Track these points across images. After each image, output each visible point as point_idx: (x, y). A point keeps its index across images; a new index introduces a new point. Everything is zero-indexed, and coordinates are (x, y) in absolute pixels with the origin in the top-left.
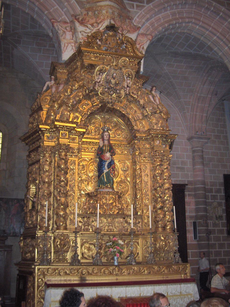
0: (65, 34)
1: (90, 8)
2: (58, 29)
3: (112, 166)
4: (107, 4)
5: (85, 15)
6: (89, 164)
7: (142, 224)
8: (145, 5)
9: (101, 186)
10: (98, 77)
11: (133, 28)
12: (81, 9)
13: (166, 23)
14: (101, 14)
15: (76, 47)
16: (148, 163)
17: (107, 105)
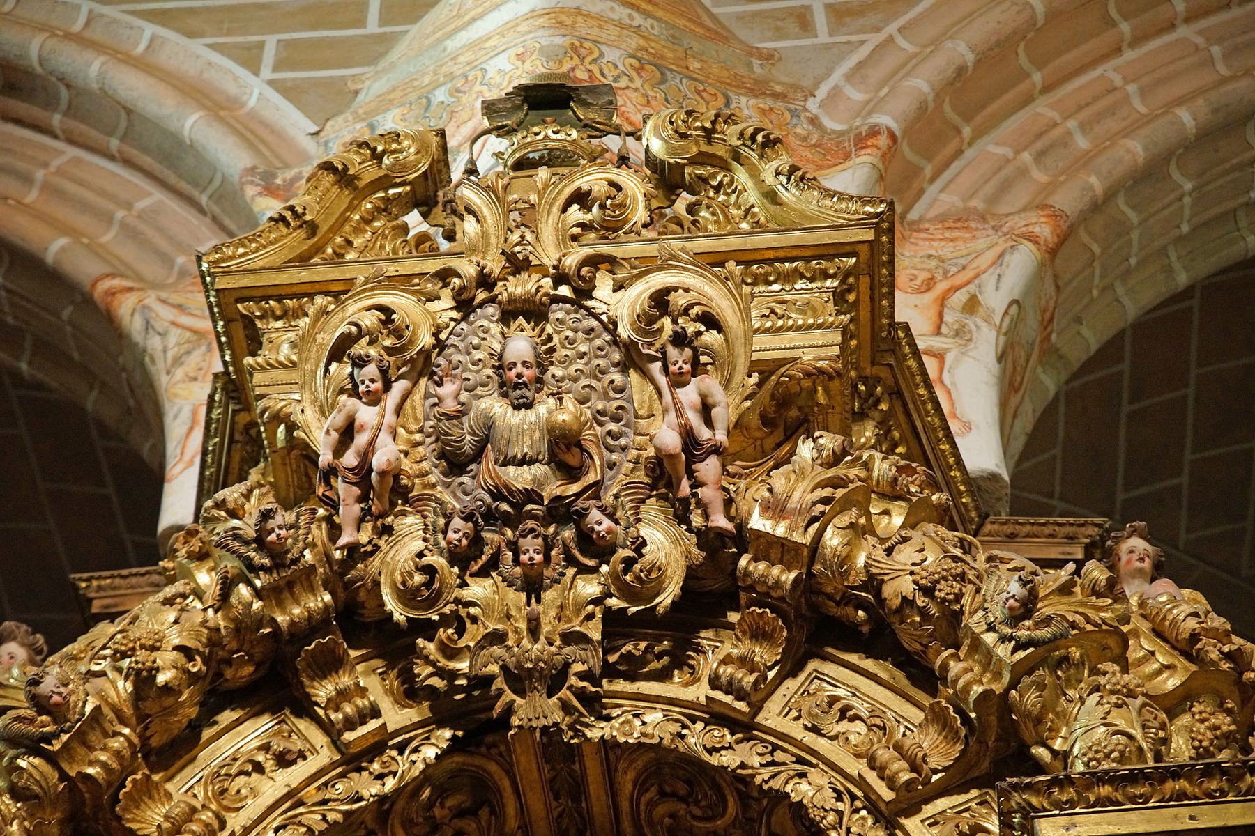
2: (148, 326)
10: (337, 419)
17: (509, 710)
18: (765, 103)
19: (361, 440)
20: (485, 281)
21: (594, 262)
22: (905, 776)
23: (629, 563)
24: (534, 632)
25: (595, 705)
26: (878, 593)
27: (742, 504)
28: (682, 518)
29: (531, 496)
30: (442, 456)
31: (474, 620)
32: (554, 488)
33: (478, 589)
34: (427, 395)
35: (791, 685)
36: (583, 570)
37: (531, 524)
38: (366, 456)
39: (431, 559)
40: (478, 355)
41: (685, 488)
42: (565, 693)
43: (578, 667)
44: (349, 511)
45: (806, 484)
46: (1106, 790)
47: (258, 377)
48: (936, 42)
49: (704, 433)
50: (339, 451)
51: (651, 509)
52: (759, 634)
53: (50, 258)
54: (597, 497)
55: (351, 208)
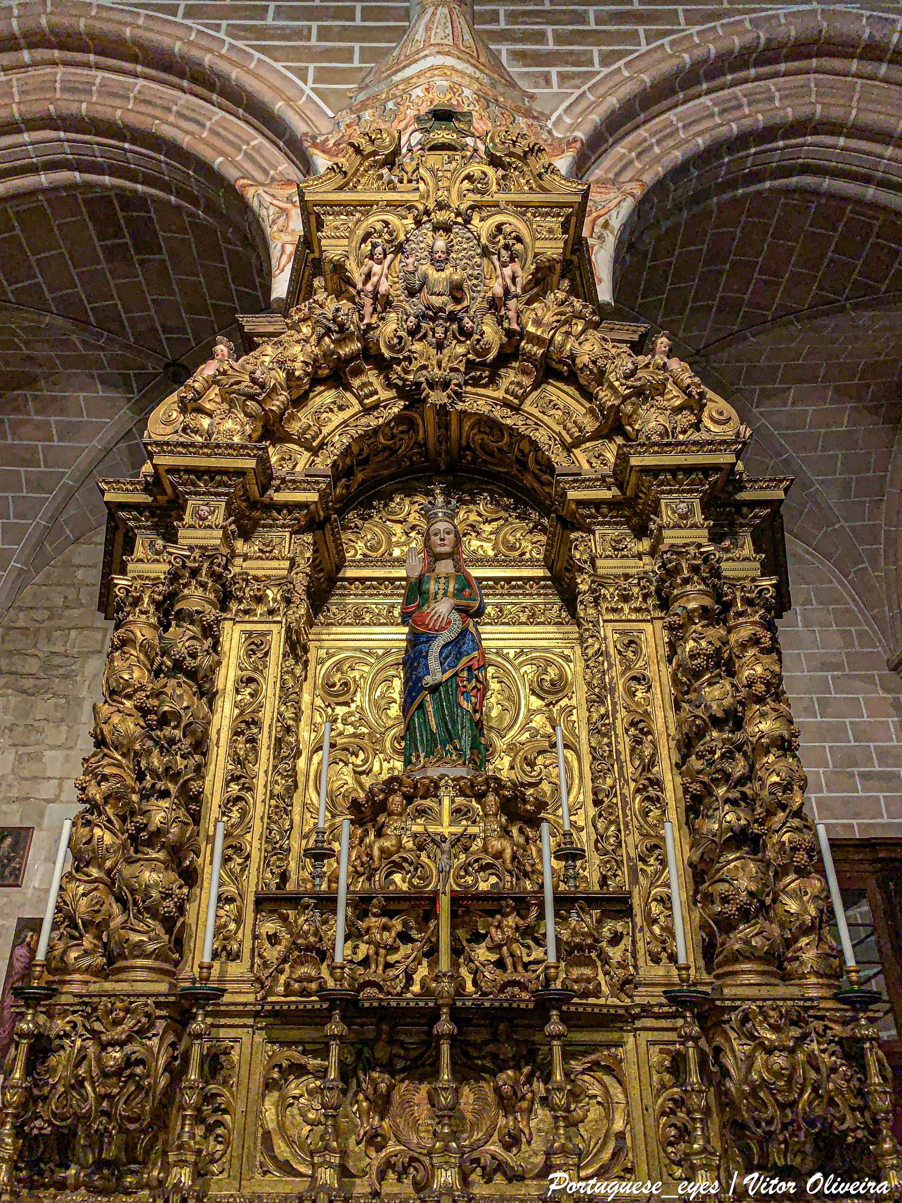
2: (260, 204)
3: (465, 660)
6: (377, 673)
7: (634, 942)
9: (414, 760)
10: (365, 269)
16: (648, 621)
17: (428, 396)
18: (530, 121)
19: (374, 279)
20: (427, 212)
21: (472, 208)
22: (577, 434)
23: (478, 341)
24: (440, 367)
25: (459, 396)
26: (574, 361)
27: (524, 319)
28: (500, 323)
29: (441, 310)
30: (406, 288)
31: (416, 359)
32: (450, 307)
33: (417, 347)
34: (401, 262)
35: (535, 394)
36: (459, 342)
37: (441, 321)
38: (376, 286)
39: (400, 333)
40: (422, 245)
41: (503, 312)
42: (449, 391)
43: (455, 381)
44: (368, 309)
45: (550, 314)
46: (656, 448)
47: (323, 242)
48: (604, 96)
49: (513, 289)
50: (365, 282)
51: (489, 319)
52: (525, 372)
53: (216, 166)
54: (467, 312)
55: (361, 165)
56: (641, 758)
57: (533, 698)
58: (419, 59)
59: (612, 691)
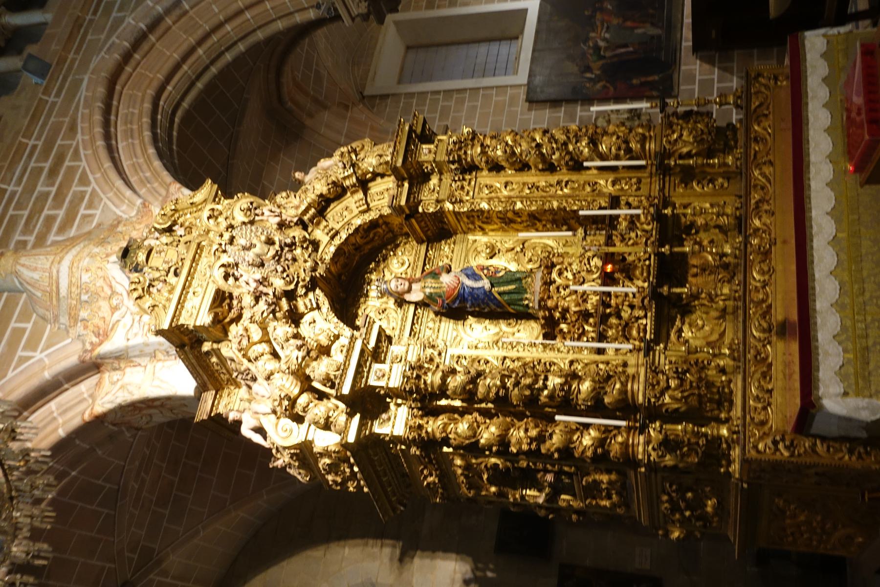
0: (130, 384)
1: (70, 314)
2: (112, 402)
3: (477, 272)
4: (67, 269)
5: (86, 327)
8: (89, 189)
9: (526, 302)
10: (244, 284)
11: (142, 217)
12: (68, 337)
13: (146, 151)
14: (91, 285)
15: (166, 358)
22: (364, 202)
32: (277, 247)
33: (292, 270)
36: (295, 249)
39: (285, 275)
40: (237, 253)
49: (277, 214)
56: (546, 187)
57: (494, 259)
58: (58, 278)
59: (510, 197)
